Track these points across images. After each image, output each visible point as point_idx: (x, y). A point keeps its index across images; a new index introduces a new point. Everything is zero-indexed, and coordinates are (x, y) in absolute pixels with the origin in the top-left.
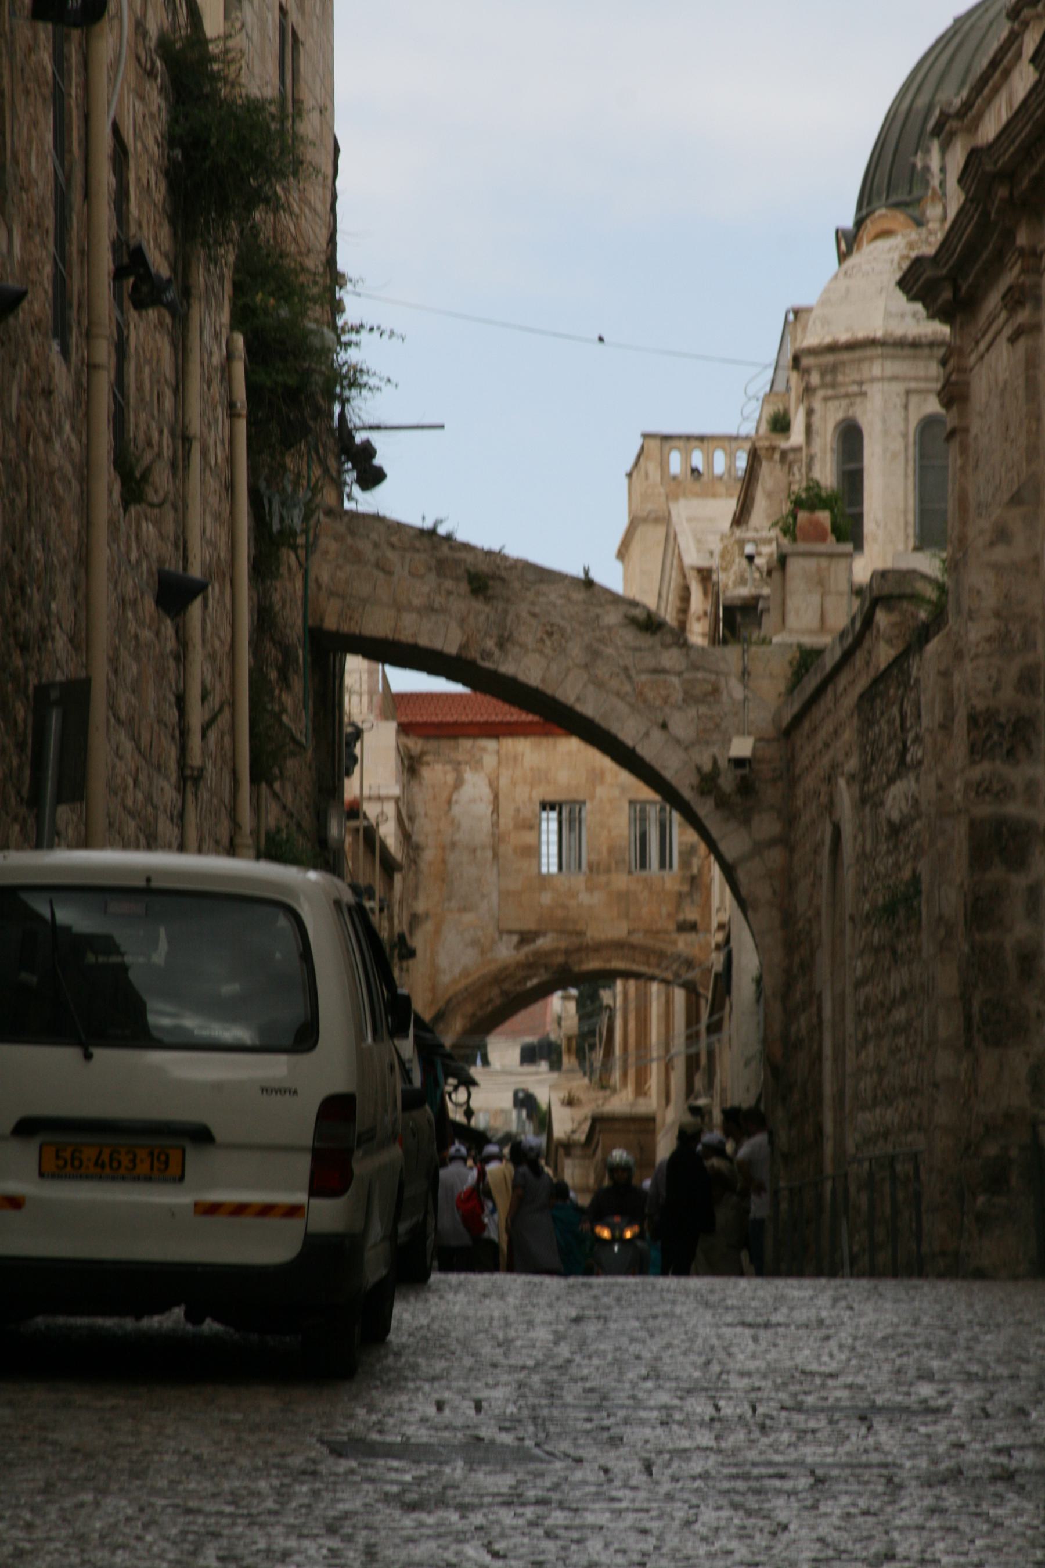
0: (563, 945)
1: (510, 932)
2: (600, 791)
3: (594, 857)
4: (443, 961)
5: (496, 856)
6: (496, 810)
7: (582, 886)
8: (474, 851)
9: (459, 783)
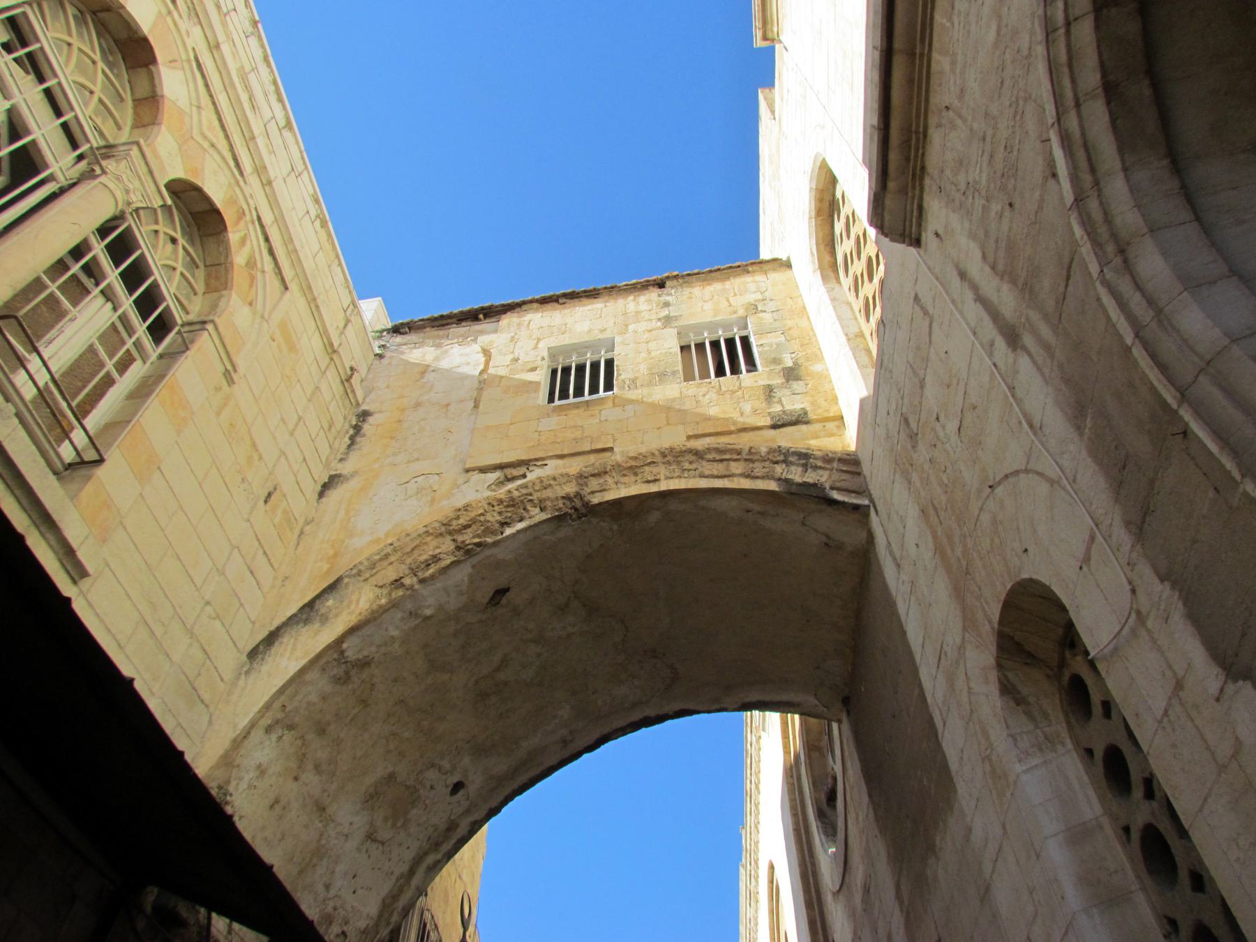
1: (483, 470)
8: (448, 405)
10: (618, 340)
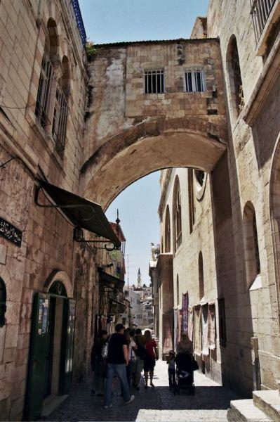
0: (155, 122)
1: (130, 117)
2: (170, 63)
3: (168, 86)
4: (99, 131)
5: (125, 89)
6: (125, 73)
7: (164, 98)
8: (115, 87)
9: (110, 64)
10: (166, 68)
